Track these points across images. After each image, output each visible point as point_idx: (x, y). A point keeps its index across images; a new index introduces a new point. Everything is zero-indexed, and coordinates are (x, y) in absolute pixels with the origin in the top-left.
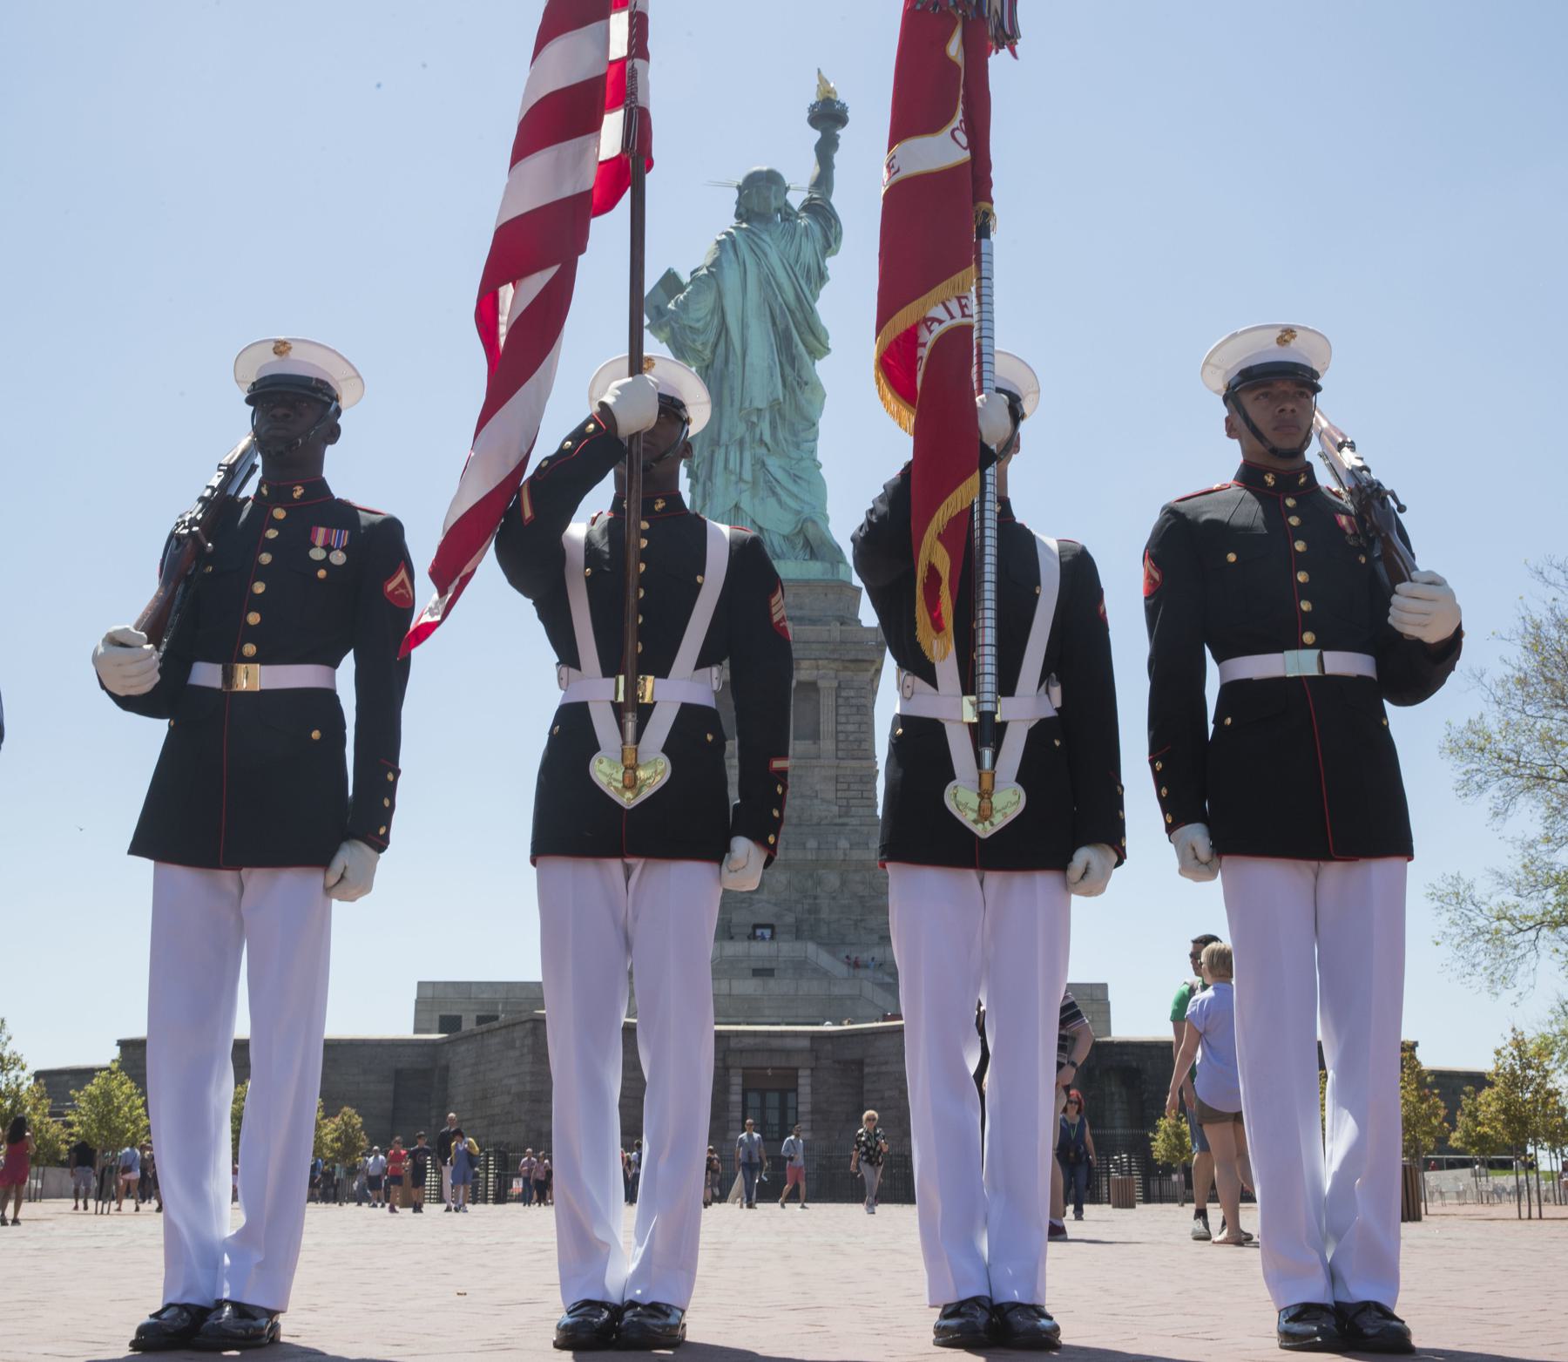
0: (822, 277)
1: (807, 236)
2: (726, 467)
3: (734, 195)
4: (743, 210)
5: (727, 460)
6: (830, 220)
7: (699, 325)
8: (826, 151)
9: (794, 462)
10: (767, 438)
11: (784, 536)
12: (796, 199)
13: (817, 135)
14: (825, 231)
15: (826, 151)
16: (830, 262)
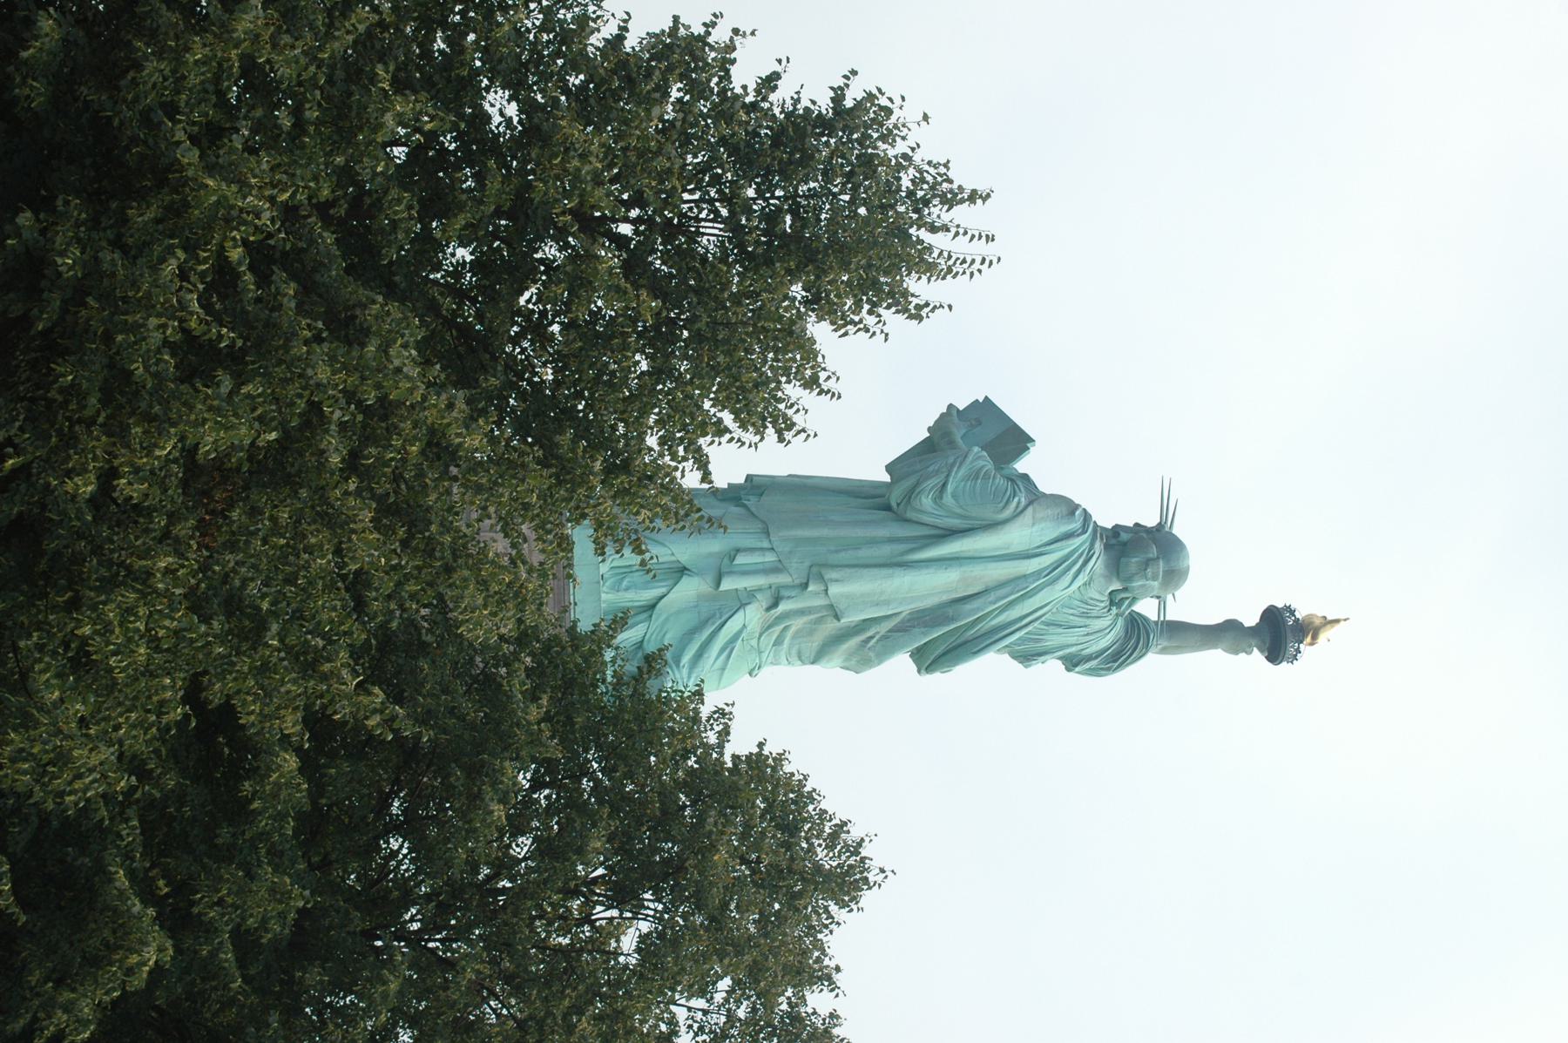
0: (1026, 657)
1: (1088, 634)
2: (738, 551)
3: (1151, 521)
4: (1124, 536)
5: (751, 550)
6: (1115, 661)
7: (948, 499)
8: (1227, 634)
9: (754, 642)
10: (783, 607)
11: (642, 642)
12: (1147, 608)
13: (1251, 619)
14: (1096, 657)
15: (1227, 634)
16: (1054, 666)
